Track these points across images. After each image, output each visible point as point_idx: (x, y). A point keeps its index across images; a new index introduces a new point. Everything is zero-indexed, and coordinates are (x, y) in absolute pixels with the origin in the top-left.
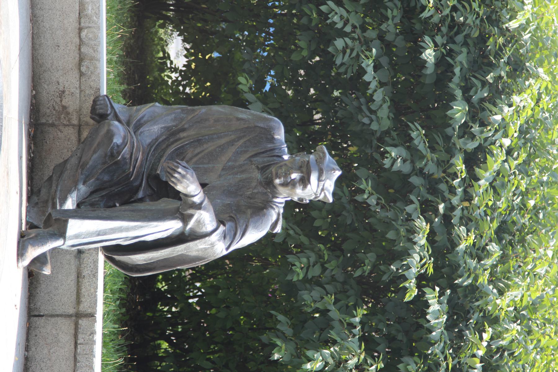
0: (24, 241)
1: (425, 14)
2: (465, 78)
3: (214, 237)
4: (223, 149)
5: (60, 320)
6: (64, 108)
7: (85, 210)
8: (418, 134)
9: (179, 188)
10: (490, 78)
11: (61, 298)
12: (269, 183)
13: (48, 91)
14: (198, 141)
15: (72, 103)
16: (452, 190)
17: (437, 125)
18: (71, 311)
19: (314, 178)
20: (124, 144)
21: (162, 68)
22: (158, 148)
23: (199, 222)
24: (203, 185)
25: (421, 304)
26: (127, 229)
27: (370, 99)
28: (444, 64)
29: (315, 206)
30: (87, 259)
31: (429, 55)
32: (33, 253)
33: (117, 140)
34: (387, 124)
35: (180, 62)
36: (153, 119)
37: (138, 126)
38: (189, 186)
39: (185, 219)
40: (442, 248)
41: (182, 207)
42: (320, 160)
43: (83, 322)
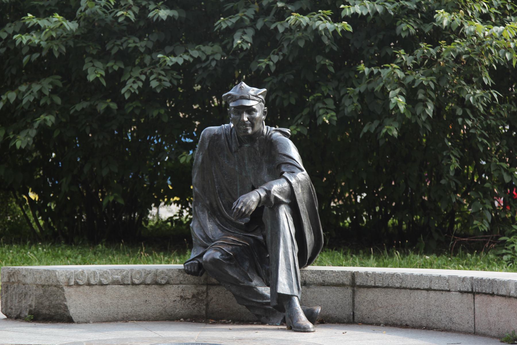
0: (293, 327)
1: (132, 17)
3: (293, 181)
5: (357, 299)
6: (193, 296)
7: (271, 280)
8: (224, 23)
9: (253, 207)
11: (338, 299)
12: (252, 138)
13: (180, 308)
15: (190, 291)
18: (350, 290)
20: (221, 250)
21: (179, 222)
23: (280, 193)
24: (253, 188)
25: (354, 19)
26: (286, 248)
27: (198, 60)
30: (310, 278)
33: (218, 255)
34: (217, 48)
35: (175, 209)
36: (202, 228)
37: (208, 239)
39: (278, 203)
41: (270, 205)
42: (233, 98)
43: (358, 282)
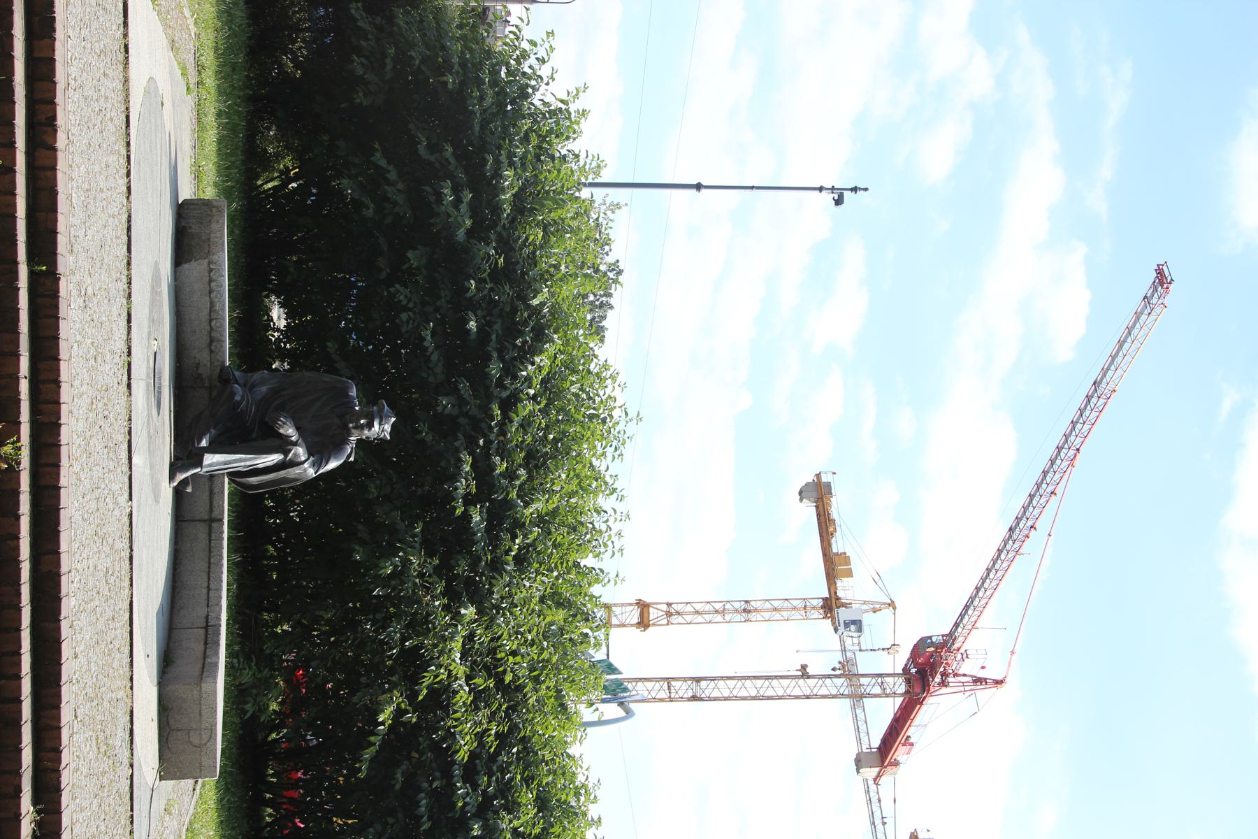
0: (174, 470)
2: (499, 340)
16: (491, 428)
17: (480, 379)
30: (217, 482)
32: (181, 477)
39: (286, 453)
40: (483, 470)
41: (283, 445)
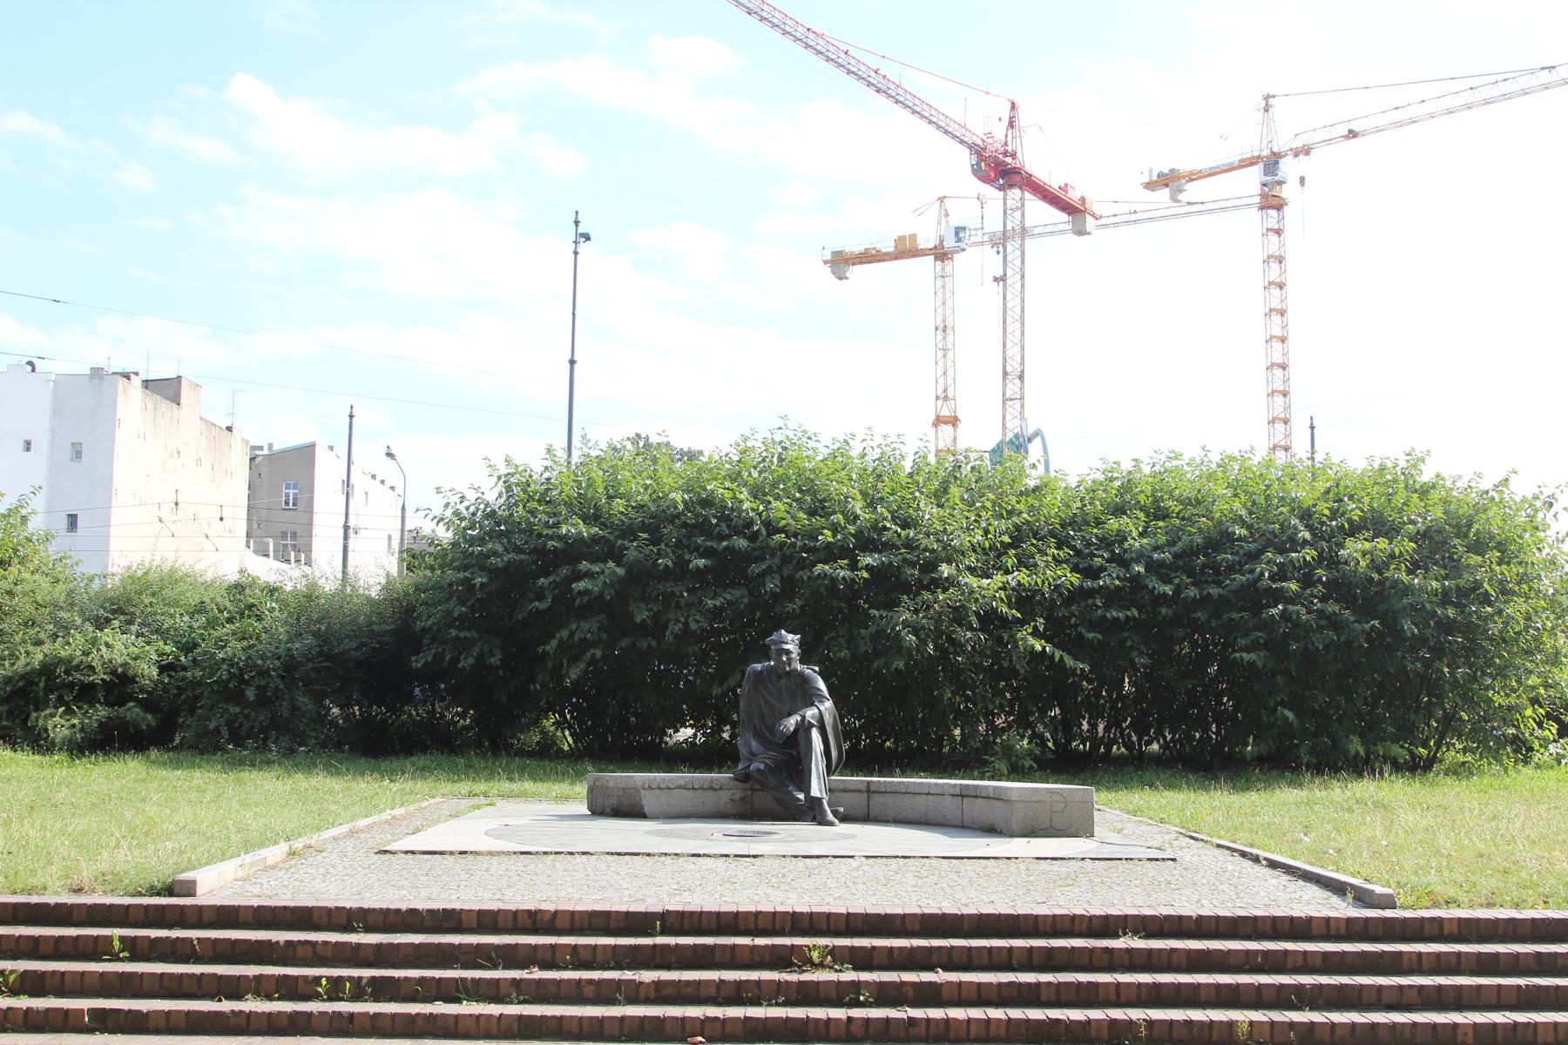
0: (823, 822)
2: (712, 539)
4: (767, 703)
7: (805, 786)
10: (714, 521)
12: (788, 674)
13: (730, 809)
14: (762, 717)
16: (793, 545)
17: (747, 557)
19: (786, 647)
22: (766, 743)
24: (790, 715)
28: (707, 553)
29: (802, 644)
30: (834, 786)
31: (701, 562)
32: (830, 817)
38: (792, 722)
39: (811, 725)
40: (830, 554)
41: (804, 728)
